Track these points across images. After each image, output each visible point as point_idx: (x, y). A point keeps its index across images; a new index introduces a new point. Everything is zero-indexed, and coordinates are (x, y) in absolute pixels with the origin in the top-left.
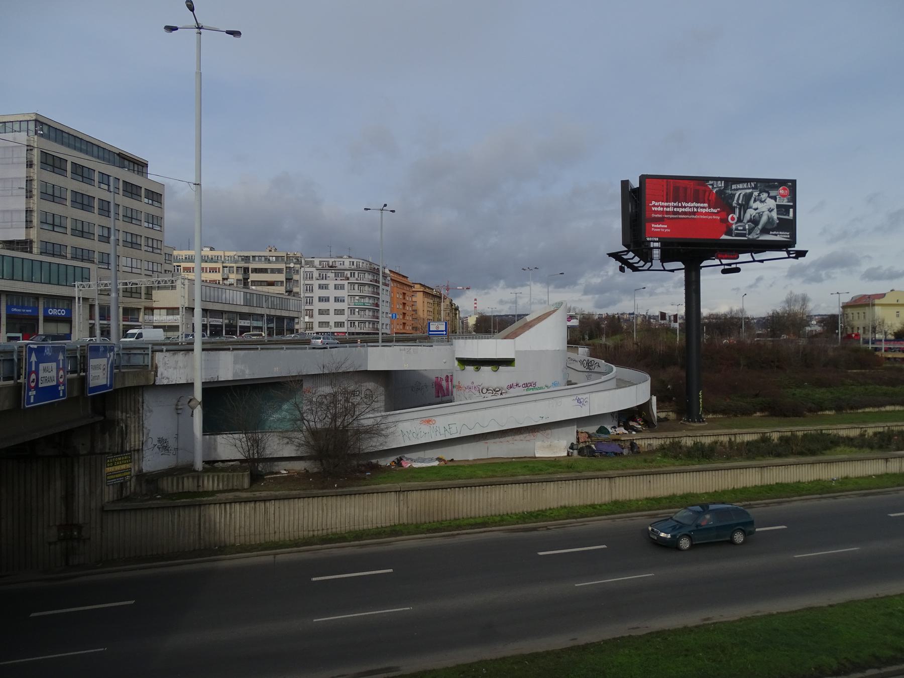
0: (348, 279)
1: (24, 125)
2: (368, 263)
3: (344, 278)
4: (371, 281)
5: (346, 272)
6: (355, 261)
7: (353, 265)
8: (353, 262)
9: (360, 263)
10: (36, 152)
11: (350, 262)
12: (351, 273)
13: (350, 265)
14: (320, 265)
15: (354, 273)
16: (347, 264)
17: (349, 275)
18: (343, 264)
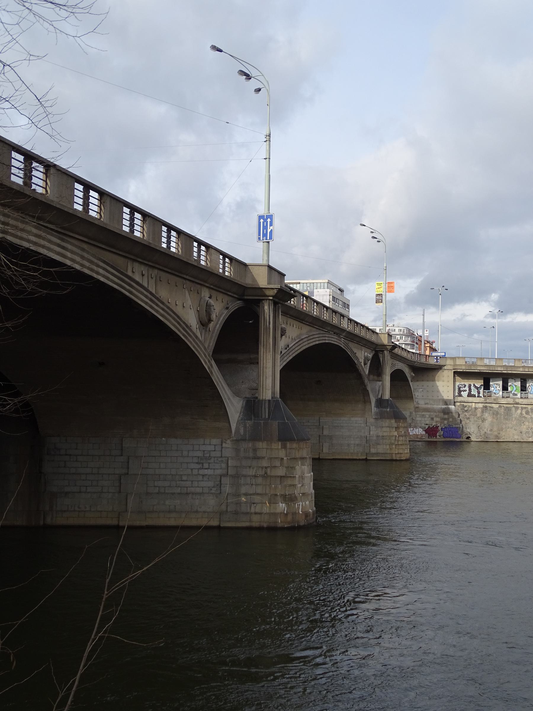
0: (399, 341)
1: (322, 284)
2: (408, 330)
3: (396, 340)
4: (411, 342)
5: (397, 336)
6: (402, 329)
7: (401, 331)
8: (401, 330)
9: (405, 330)
10: (331, 297)
11: (399, 329)
12: (400, 337)
13: (399, 331)
14: (380, 331)
15: (402, 337)
16: (397, 332)
17: (399, 338)
18: (395, 331)
